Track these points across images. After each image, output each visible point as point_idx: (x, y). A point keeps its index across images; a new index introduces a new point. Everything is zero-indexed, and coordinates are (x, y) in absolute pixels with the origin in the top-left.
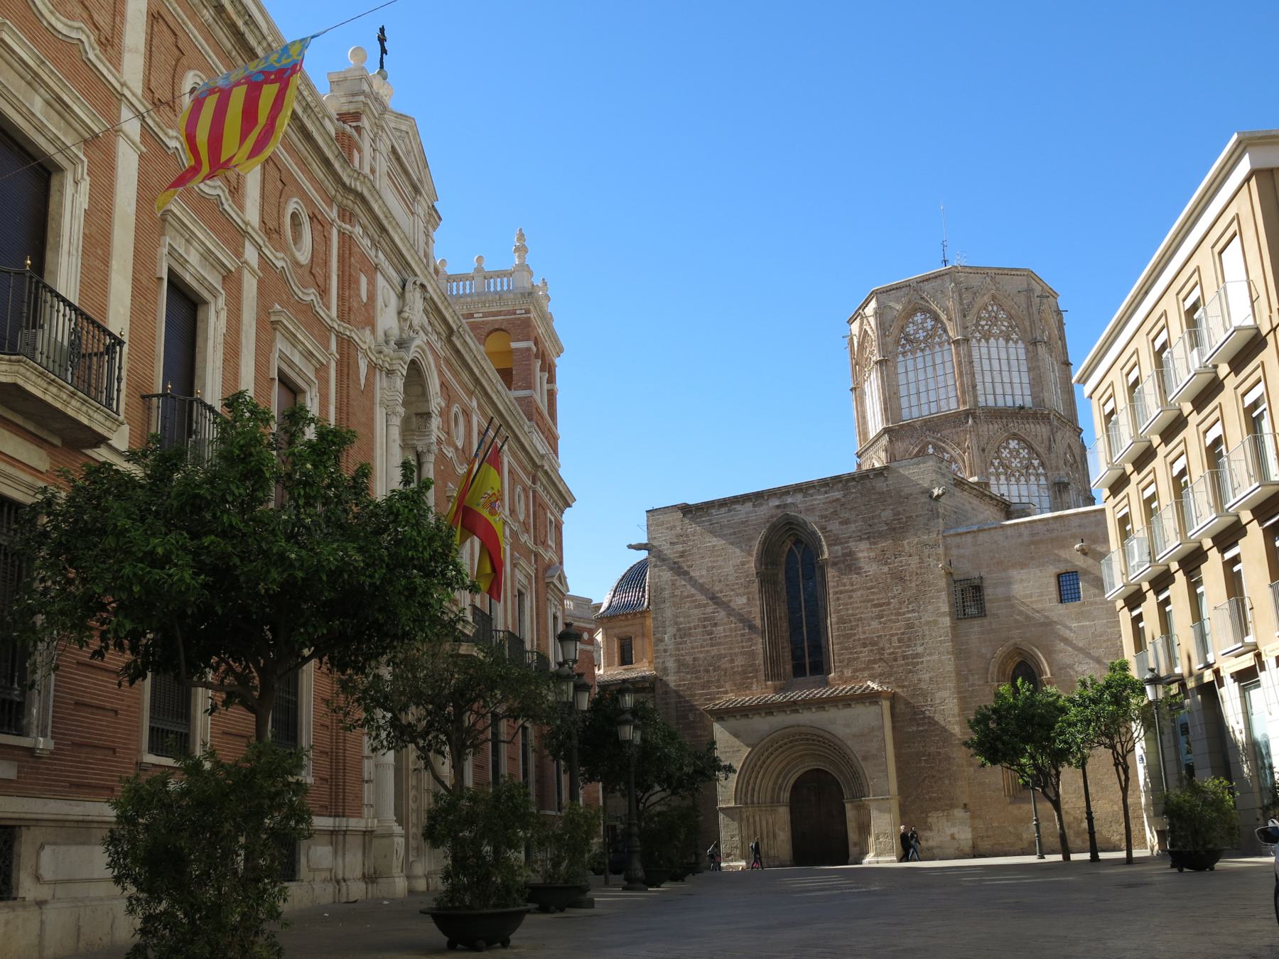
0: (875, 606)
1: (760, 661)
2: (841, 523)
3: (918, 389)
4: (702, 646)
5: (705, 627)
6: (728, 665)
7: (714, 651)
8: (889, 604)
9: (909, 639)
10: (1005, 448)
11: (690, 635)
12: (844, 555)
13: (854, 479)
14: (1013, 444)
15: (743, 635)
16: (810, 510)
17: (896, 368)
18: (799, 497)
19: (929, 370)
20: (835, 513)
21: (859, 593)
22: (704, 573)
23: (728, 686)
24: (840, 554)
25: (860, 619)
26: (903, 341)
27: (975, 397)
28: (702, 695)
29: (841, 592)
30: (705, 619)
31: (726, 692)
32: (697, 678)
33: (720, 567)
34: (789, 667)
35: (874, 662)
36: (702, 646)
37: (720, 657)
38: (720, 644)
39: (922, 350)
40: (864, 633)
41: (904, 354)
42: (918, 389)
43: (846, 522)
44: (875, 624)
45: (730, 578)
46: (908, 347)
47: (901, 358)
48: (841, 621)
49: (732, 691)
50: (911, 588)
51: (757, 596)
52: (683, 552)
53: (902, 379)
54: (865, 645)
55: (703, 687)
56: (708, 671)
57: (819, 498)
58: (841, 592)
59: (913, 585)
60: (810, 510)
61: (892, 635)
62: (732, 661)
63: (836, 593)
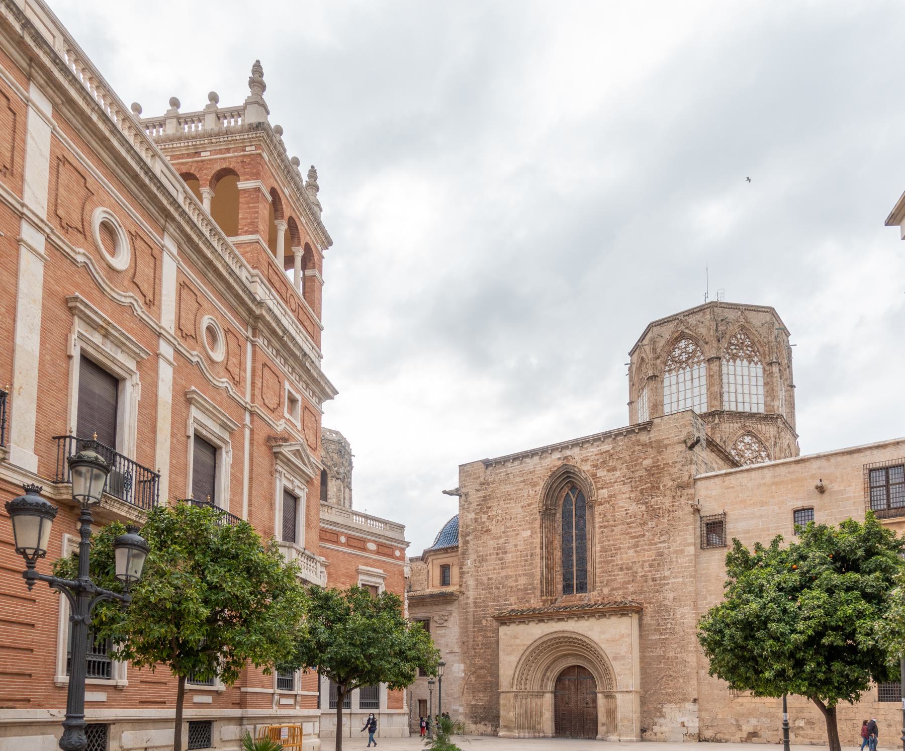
0: (632, 538)
1: (537, 582)
2: (609, 471)
3: (678, 398)
4: (495, 569)
5: (497, 554)
7: (504, 573)
8: (644, 535)
9: (659, 565)
10: (741, 442)
12: (610, 496)
13: (621, 434)
14: (747, 439)
15: (526, 561)
16: (585, 460)
17: (662, 382)
18: (576, 450)
19: (688, 383)
20: (604, 462)
21: (619, 528)
24: (606, 496)
25: (620, 549)
26: (670, 362)
27: (721, 402)
29: (605, 527)
34: (560, 587)
35: (628, 583)
36: (495, 569)
37: (507, 577)
38: (508, 567)
39: (684, 369)
40: (622, 559)
41: (670, 370)
42: (678, 398)
43: (614, 469)
44: (631, 552)
46: (673, 367)
47: (667, 375)
48: (604, 550)
50: (663, 523)
51: (538, 530)
53: (666, 391)
54: (621, 569)
57: (592, 451)
58: (605, 527)
59: (666, 520)
60: (585, 460)
61: (644, 561)
62: (517, 580)
63: (601, 527)
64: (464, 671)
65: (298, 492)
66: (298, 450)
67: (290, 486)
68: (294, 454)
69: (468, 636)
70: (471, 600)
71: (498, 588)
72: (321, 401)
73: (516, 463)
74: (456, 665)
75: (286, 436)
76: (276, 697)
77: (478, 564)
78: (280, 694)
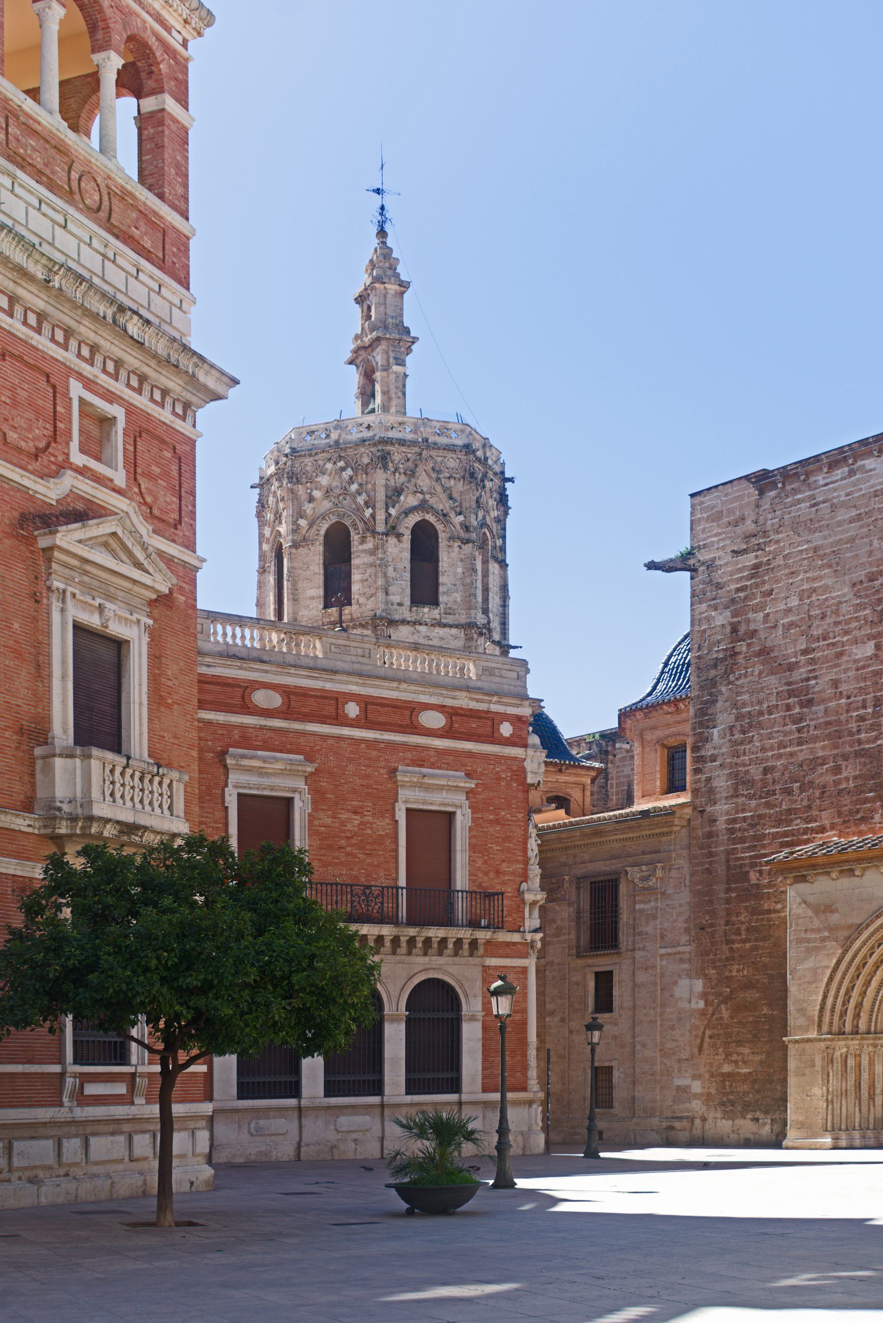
4: (782, 745)
5: (788, 708)
6: (830, 778)
7: (804, 753)
11: (760, 725)
22: (794, 602)
23: (826, 818)
28: (775, 836)
30: (791, 694)
31: (822, 829)
32: (768, 805)
33: (826, 589)
36: (782, 745)
37: (815, 763)
38: (815, 739)
45: (844, 608)
49: (832, 827)
52: (756, 566)
55: (779, 823)
56: (788, 792)
62: (837, 770)
64: (704, 996)
65: (116, 629)
66: (114, 534)
67: (93, 620)
68: (106, 545)
69: (713, 913)
70: (721, 824)
71: (788, 792)
72: (187, 409)
73: (839, 473)
74: (684, 982)
75: (80, 506)
76: (69, 1081)
77: (738, 736)
78: (82, 1074)
